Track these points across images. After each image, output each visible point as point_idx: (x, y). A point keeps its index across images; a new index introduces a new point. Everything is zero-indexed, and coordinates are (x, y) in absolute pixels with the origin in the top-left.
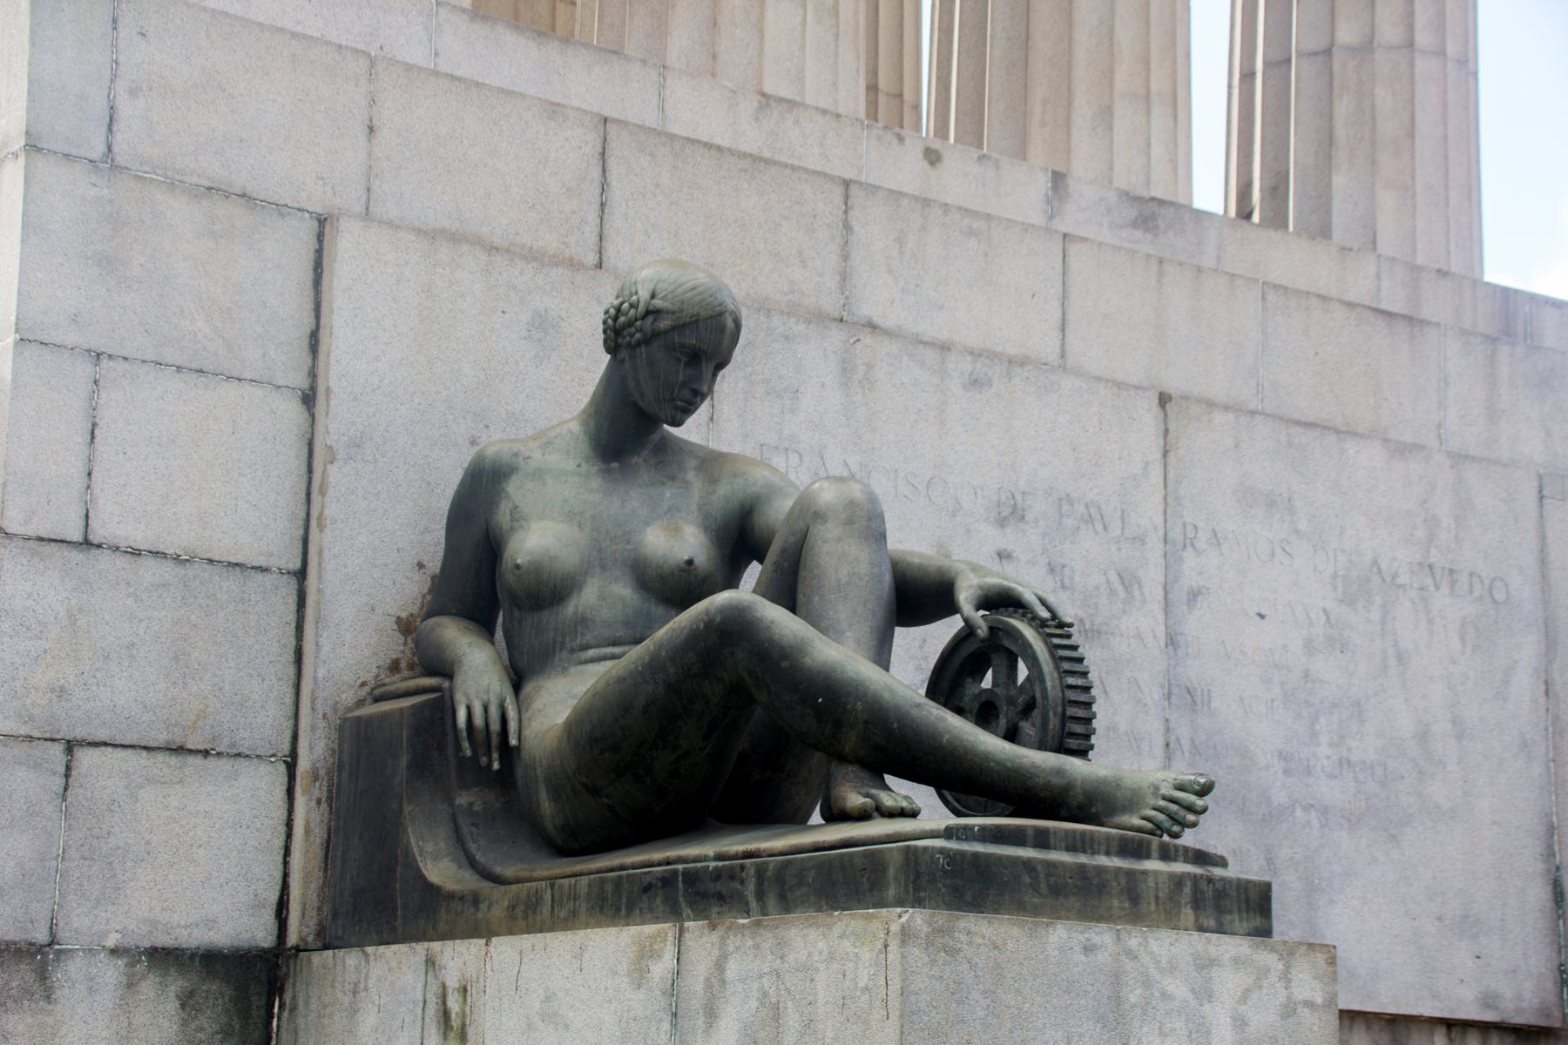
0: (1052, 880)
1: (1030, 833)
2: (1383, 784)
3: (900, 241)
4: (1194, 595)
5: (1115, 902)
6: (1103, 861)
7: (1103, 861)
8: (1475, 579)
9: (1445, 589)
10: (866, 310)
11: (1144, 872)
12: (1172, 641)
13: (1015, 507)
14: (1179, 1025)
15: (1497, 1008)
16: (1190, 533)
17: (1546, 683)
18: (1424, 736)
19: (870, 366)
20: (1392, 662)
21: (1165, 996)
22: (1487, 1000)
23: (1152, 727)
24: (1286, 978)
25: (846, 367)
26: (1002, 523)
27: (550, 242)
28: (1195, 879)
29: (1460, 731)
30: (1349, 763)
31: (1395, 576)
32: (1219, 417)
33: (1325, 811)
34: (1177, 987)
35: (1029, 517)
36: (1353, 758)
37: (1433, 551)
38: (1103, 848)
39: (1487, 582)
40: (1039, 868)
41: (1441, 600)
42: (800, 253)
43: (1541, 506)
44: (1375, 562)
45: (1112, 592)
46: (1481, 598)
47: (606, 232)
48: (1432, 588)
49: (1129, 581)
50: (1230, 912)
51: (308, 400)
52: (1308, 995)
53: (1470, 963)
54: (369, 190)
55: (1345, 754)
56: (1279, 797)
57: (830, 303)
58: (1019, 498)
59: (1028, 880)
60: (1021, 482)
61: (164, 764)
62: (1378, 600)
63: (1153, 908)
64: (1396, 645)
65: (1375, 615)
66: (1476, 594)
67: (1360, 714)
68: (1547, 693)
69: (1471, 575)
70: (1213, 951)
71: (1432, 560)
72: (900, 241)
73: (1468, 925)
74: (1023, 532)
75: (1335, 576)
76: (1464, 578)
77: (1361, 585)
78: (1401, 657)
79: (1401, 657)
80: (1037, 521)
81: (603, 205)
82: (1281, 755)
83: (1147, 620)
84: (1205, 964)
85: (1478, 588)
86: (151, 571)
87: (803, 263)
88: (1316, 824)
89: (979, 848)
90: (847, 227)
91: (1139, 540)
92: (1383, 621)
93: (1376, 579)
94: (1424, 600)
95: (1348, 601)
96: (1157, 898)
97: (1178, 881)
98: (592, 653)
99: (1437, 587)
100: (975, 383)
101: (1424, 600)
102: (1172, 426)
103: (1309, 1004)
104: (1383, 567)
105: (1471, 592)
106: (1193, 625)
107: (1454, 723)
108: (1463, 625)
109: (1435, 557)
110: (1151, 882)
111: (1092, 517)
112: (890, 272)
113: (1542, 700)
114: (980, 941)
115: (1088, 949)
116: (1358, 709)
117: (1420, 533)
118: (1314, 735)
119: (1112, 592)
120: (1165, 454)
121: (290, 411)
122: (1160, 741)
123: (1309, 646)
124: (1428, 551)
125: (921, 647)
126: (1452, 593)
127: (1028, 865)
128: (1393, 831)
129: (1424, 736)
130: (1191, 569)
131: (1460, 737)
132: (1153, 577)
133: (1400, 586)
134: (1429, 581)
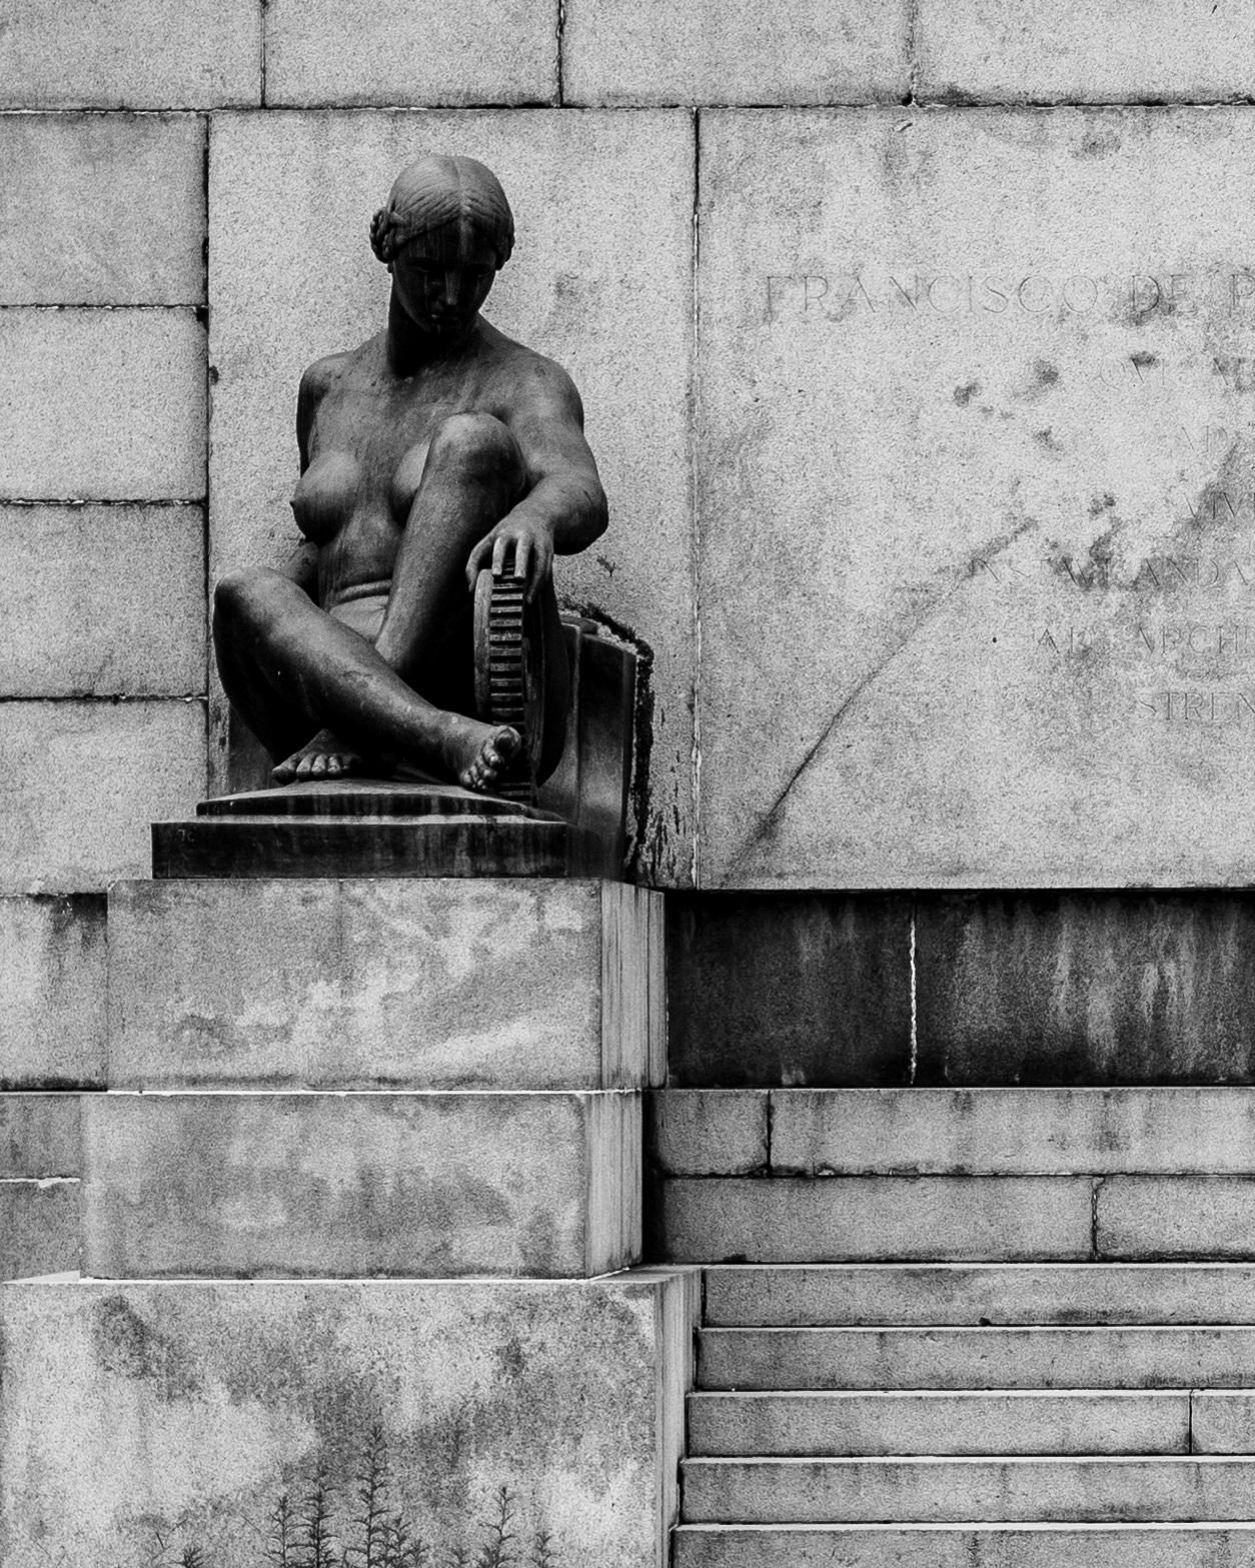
0: (306, 842)
1: (291, 802)
5: (378, 856)
6: (372, 820)
7: (372, 820)
10: (946, 75)
11: (415, 828)
13: (1158, 298)
14: (411, 958)
19: (926, 155)
21: (393, 933)
24: (539, 910)
25: (890, 160)
26: (1138, 320)
27: (491, 83)
28: (473, 829)
34: (408, 927)
35: (1183, 306)
38: (375, 809)
40: (292, 833)
42: (844, 24)
47: (566, 54)
50: (515, 855)
51: (202, 315)
52: (565, 924)
54: (264, 70)
57: (892, 77)
58: (1166, 284)
59: (279, 844)
60: (1170, 262)
61: (69, 714)
63: (422, 856)
70: (451, 893)
74: (1174, 327)
80: (1195, 309)
81: (561, 24)
84: (440, 905)
86: (45, 521)
87: (849, 36)
89: (229, 820)
96: (427, 849)
97: (453, 832)
98: (349, 591)
100: (1092, 147)
103: (567, 932)
110: (420, 835)
112: (981, 20)
114: (189, 901)
115: (305, 901)
121: (182, 327)
125: (1013, 492)
127: (281, 831)
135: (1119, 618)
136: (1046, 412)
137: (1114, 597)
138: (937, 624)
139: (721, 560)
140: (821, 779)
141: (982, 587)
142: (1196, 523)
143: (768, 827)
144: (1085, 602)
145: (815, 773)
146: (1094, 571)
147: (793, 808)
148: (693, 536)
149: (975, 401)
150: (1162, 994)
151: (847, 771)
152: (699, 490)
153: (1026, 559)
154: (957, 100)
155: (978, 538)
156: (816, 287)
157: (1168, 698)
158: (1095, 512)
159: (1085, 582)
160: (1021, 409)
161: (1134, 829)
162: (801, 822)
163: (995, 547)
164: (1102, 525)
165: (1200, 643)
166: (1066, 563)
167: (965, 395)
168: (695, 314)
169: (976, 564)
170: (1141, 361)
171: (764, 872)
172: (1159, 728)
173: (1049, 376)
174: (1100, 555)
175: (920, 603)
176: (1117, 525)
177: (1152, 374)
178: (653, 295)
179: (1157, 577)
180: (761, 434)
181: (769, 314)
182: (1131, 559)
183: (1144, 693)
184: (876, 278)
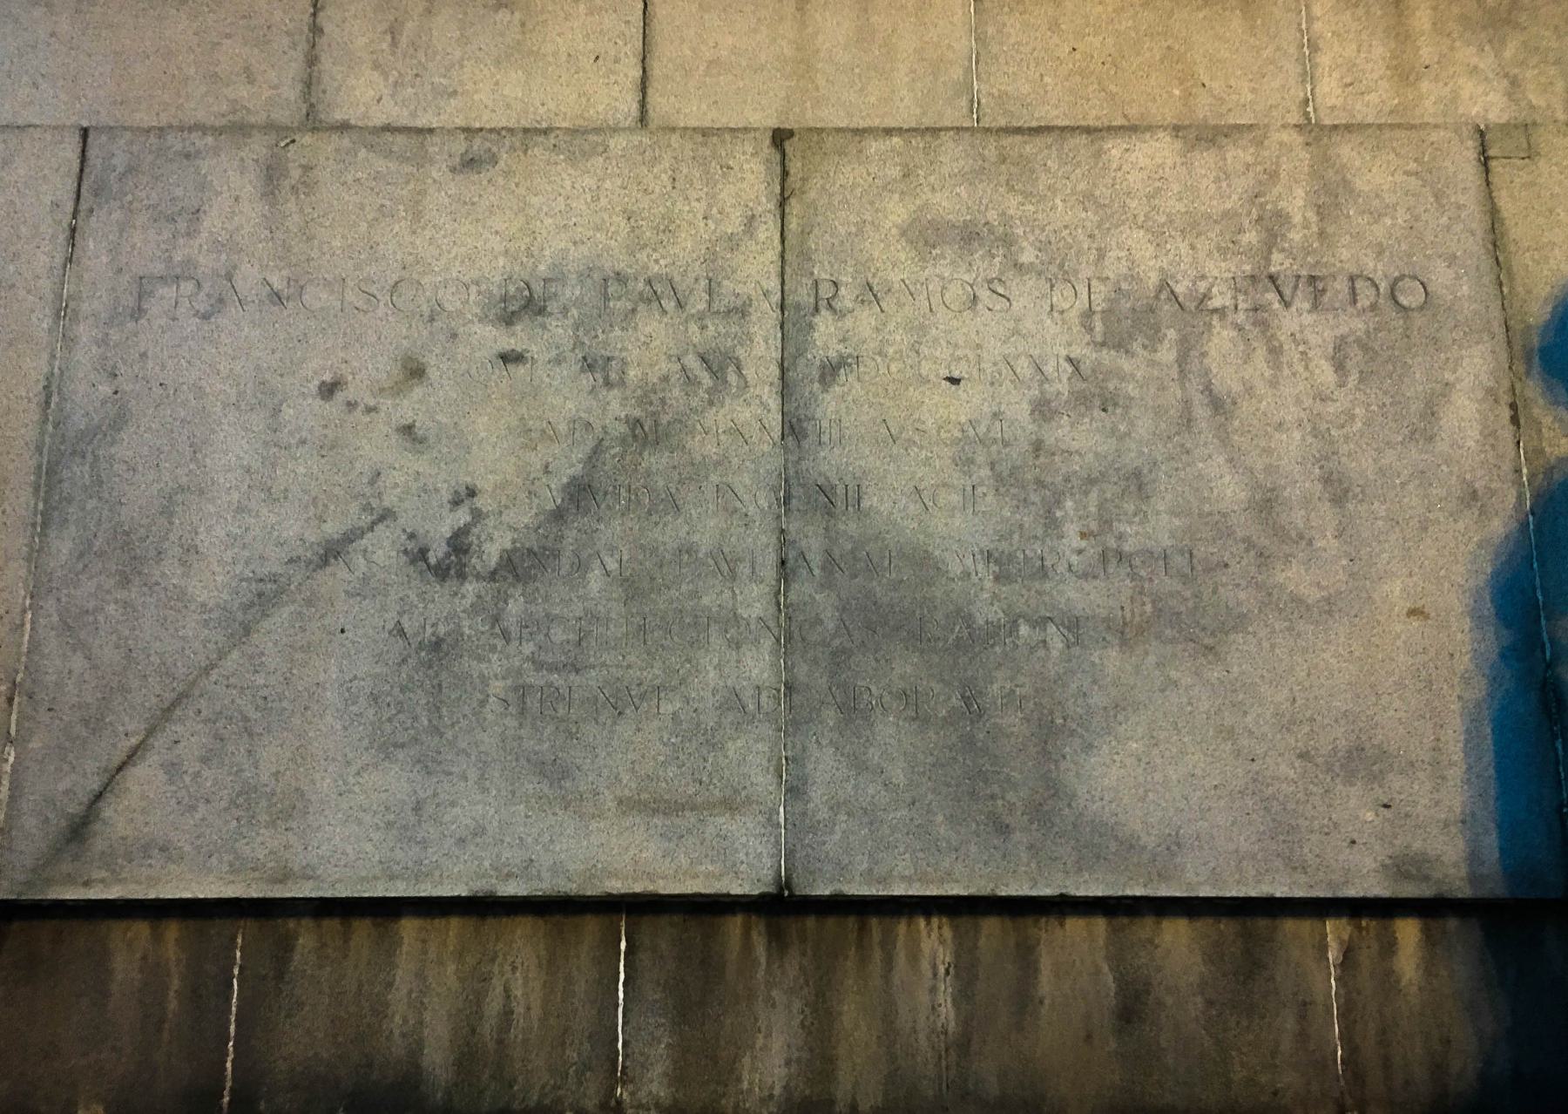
2: (1185, 579)
3: (393, 32)
4: (830, 371)
8: (1359, 284)
9: (1302, 303)
12: (794, 429)
13: (530, 299)
15: (1427, 878)
16: (826, 291)
17: (1513, 406)
18: (1266, 504)
19: (307, 168)
20: (1201, 412)
22: (1400, 867)
23: (760, 543)
25: (272, 174)
26: (508, 320)
29: (1338, 489)
30: (1120, 556)
31: (1207, 296)
32: (874, 146)
33: (1073, 625)
35: (553, 307)
36: (1127, 548)
37: (1276, 257)
39: (1383, 286)
41: (1295, 320)
42: (247, 70)
43: (1487, 171)
44: (1164, 285)
45: (690, 381)
46: (1374, 307)
48: (1276, 306)
49: (719, 364)
53: (1370, 816)
55: (1112, 543)
56: (987, 612)
58: (538, 288)
60: (542, 268)
62: (1172, 334)
64: (1208, 389)
65: (1167, 354)
66: (1364, 302)
67: (1140, 488)
68: (1515, 420)
69: (1352, 279)
71: (1273, 269)
72: (393, 32)
73: (1361, 761)
74: (544, 327)
75: (1089, 313)
76: (1341, 285)
77: (1129, 320)
78: (1217, 404)
79: (1217, 404)
80: (565, 311)
82: (989, 556)
83: (754, 408)
85: (1366, 297)
87: (251, 80)
88: (1057, 644)
90: (316, 29)
91: (741, 311)
92: (1182, 360)
93: (1167, 308)
94: (1263, 325)
95: (1116, 342)
99: (1287, 305)
100: (470, 163)
101: (1263, 325)
102: (795, 167)
104: (1180, 289)
105: (1355, 301)
106: (828, 405)
107: (1327, 480)
108: (1337, 349)
109: (1279, 263)
111: (658, 293)
112: (376, 66)
113: (1507, 433)
116: (1138, 483)
117: (1251, 237)
118: (1052, 524)
119: (690, 381)
120: (783, 202)
122: (771, 558)
123: (1043, 409)
124: (1268, 260)
125: (372, 483)
126: (1315, 307)
128: (1208, 641)
129: (1266, 504)
130: (825, 335)
131: (1338, 500)
132: (761, 349)
133: (1215, 310)
134: (1271, 296)
135: (475, 610)
136: (408, 407)
137: (471, 588)
138: (282, 616)
139: (63, 547)
140: (145, 777)
141: (337, 577)
142: (558, 515)
143: (79, 830)
144: (439, 593)
145: (139, 771)
146: (453, 561)
147: (107, 811)
148: (34, 525)
149: (340, 396)
150: (507, 1013)
151: (172, 769)
152: (48, 478)
153: (383, 548)
154: (344, 127)
155: (333, 529)
156: (187, 287)
157: (522, 691)
158: (456, 503)
159: (440, 572)
160: (387, 403)
161: (480, 831)
162: (118, 819)
163: (350, 537)
164: (463, 516)
165: (558, 634)
166: (423, 553)
167: (329, 390)
168: (63, 311)
169: (332, 552)
170: (509, 358)
171: (70, 880)
172: (511, 722)
173: (415, 372)
174: (459, 544)
175: (265, 596)
176: (477, 515)
177: (521, 371)
178: (22, 293)
179: (517, 567)
180: (119, 421)
181: (138, 313)
182: (492, 552)
183: (497, 687)
184: (249, 277)
